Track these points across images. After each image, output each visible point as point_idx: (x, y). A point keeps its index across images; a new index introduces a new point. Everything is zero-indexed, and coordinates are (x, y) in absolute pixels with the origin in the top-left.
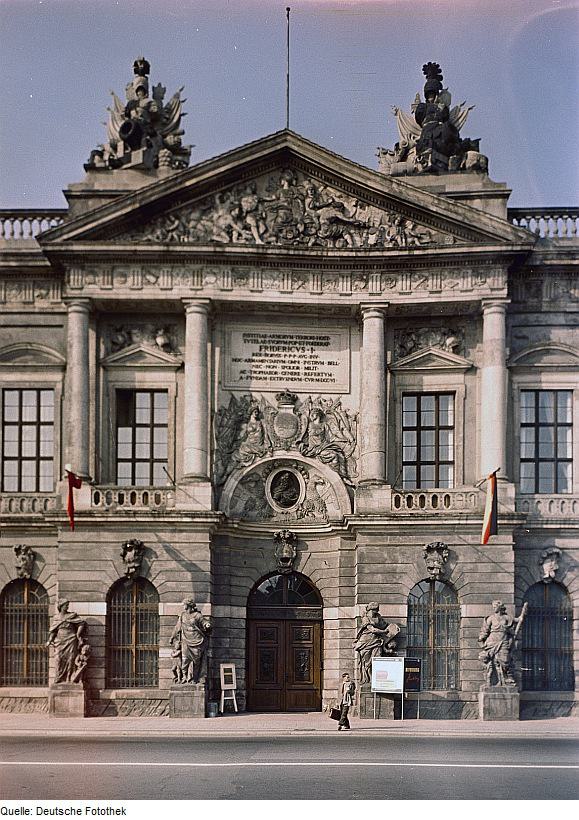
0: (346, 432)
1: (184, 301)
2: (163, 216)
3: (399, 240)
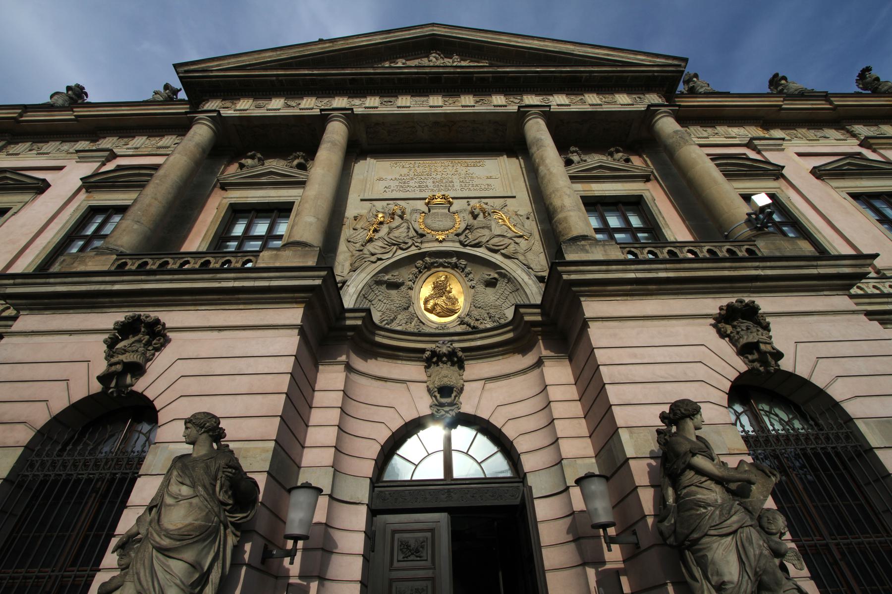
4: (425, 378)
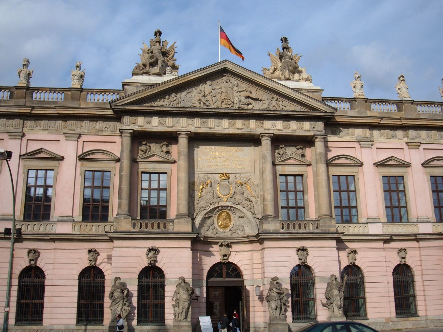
0: (253, 193)
1: (178, 132)
2: (169, 95)
3: (277, 107)
4: (219, 250)
